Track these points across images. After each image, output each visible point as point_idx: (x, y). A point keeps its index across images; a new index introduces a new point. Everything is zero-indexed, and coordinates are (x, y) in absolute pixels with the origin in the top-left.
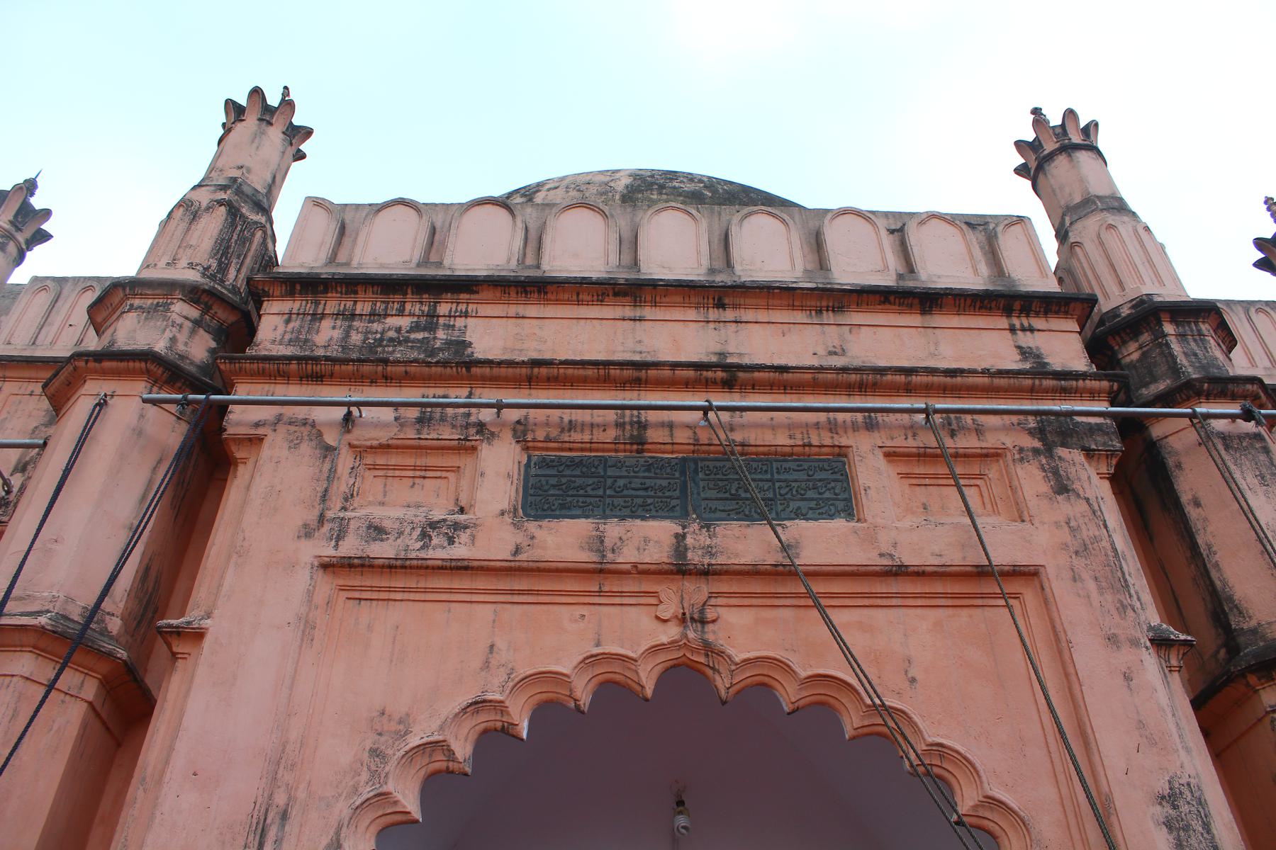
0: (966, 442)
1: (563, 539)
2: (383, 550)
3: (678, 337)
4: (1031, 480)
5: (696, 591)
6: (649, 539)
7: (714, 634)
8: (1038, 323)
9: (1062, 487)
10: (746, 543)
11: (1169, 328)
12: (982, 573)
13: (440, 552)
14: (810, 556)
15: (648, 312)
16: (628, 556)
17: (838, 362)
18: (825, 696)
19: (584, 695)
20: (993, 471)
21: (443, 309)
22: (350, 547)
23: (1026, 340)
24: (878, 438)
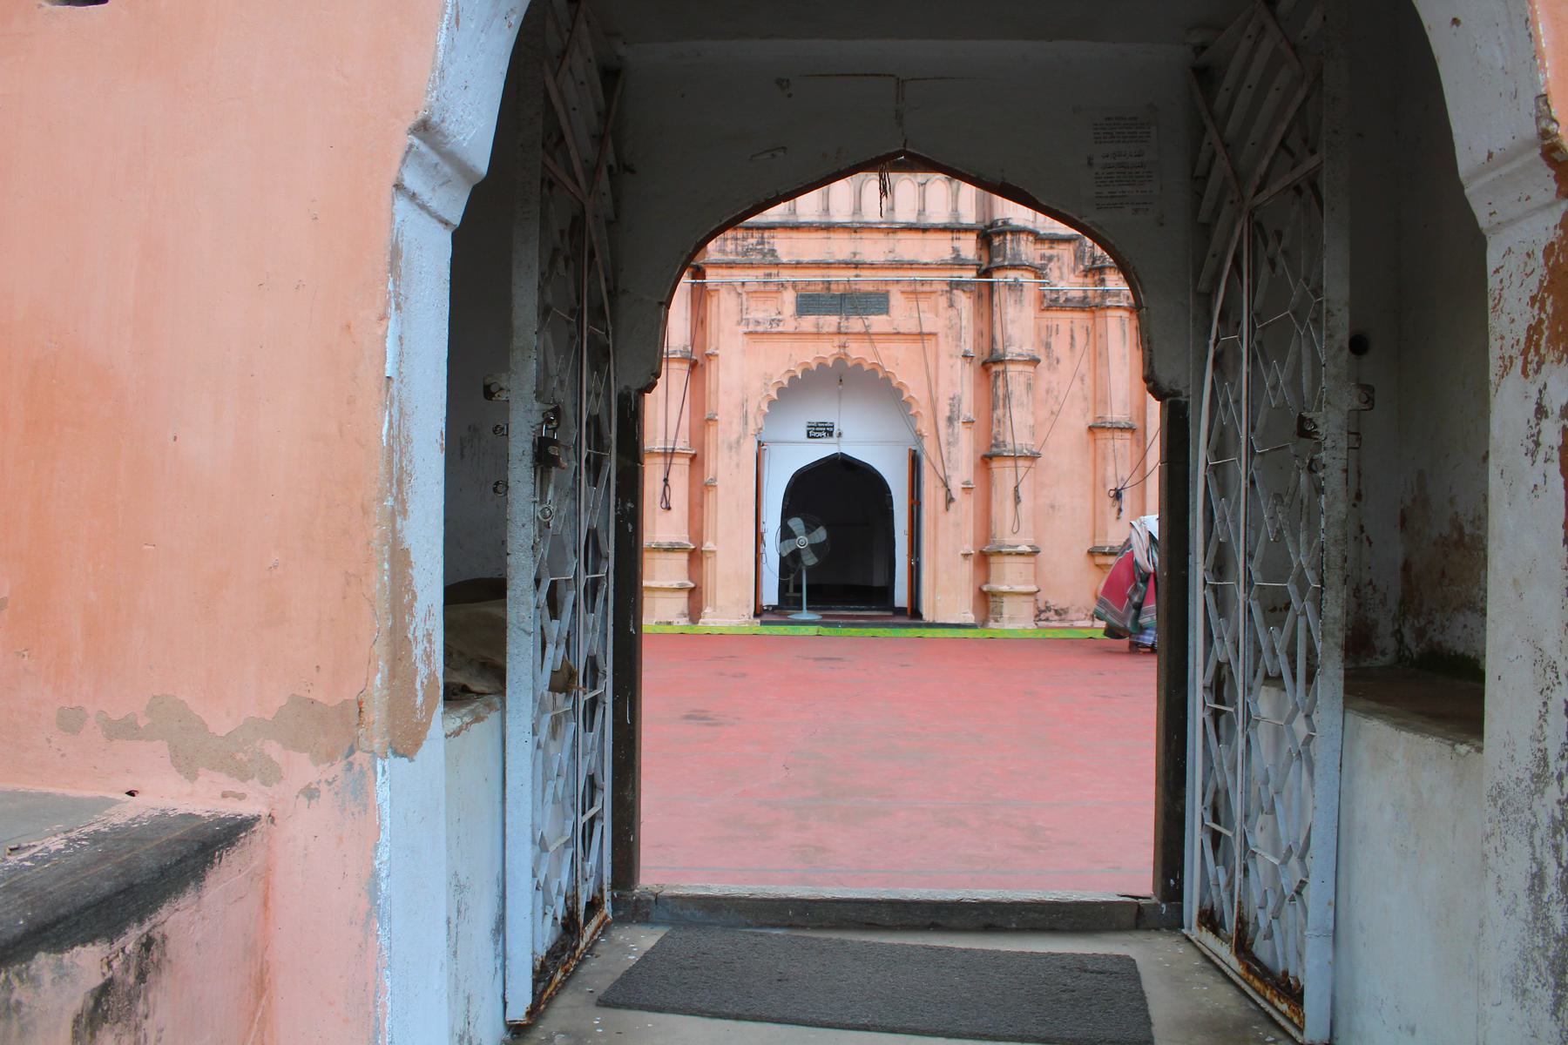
0: (927, 288)
1: (808, 323)
2: (760, 329)
3: (840, 247)
4: (943, 302)
5: (843, 338)
6: (830, 322)
7: (848, 351)
8: (962, 236)
9: (951, 306)
10: (856, 324)
11: (1009, 237)
12: (921, 334)
13: (775, 330)
14: (873, 330)
15: (832, 235)
16: (825, 330)
17: (890, 257)
18: (873, 371)
19: (814, 367)
20: (933, 297)
21: (766, 234)
22: (751, 328)
23: (956, 244)
24: (899, 287)
